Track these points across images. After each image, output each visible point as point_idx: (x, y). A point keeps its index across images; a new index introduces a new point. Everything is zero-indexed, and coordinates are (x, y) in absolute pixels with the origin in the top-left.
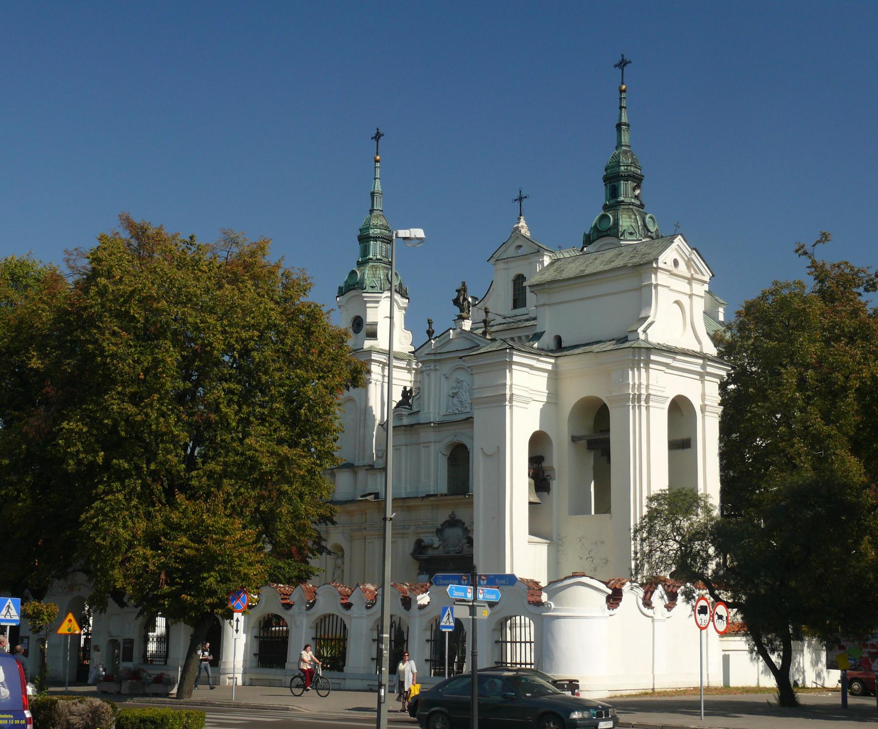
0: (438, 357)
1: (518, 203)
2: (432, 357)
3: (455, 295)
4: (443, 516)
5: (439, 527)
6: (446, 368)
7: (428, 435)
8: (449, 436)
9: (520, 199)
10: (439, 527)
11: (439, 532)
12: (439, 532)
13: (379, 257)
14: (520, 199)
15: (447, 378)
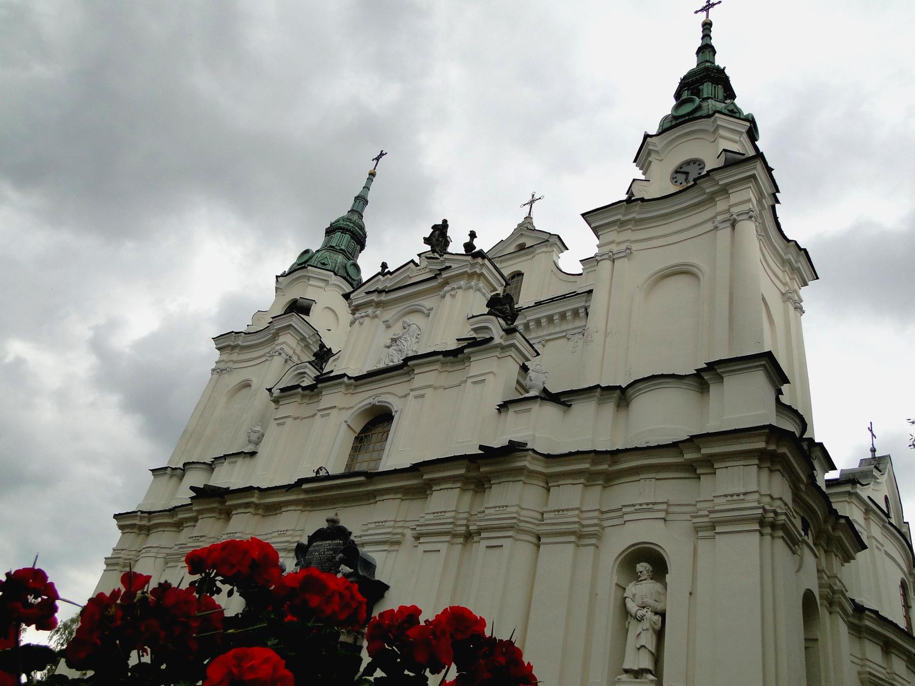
0: (383, 298)
1: (528, 207)
2: (374, 297)
3: (428, 232)
4: (317, 521)
5: (305, 541)
6: (390, 314)
7: (332, 397)
8: (367, 397)
9: (531, 202)
10: (305, 541)
11: (301, 550)
12: (301, 550)
13: (343, 247)
14: (531, 202)
15: (388, 327)
